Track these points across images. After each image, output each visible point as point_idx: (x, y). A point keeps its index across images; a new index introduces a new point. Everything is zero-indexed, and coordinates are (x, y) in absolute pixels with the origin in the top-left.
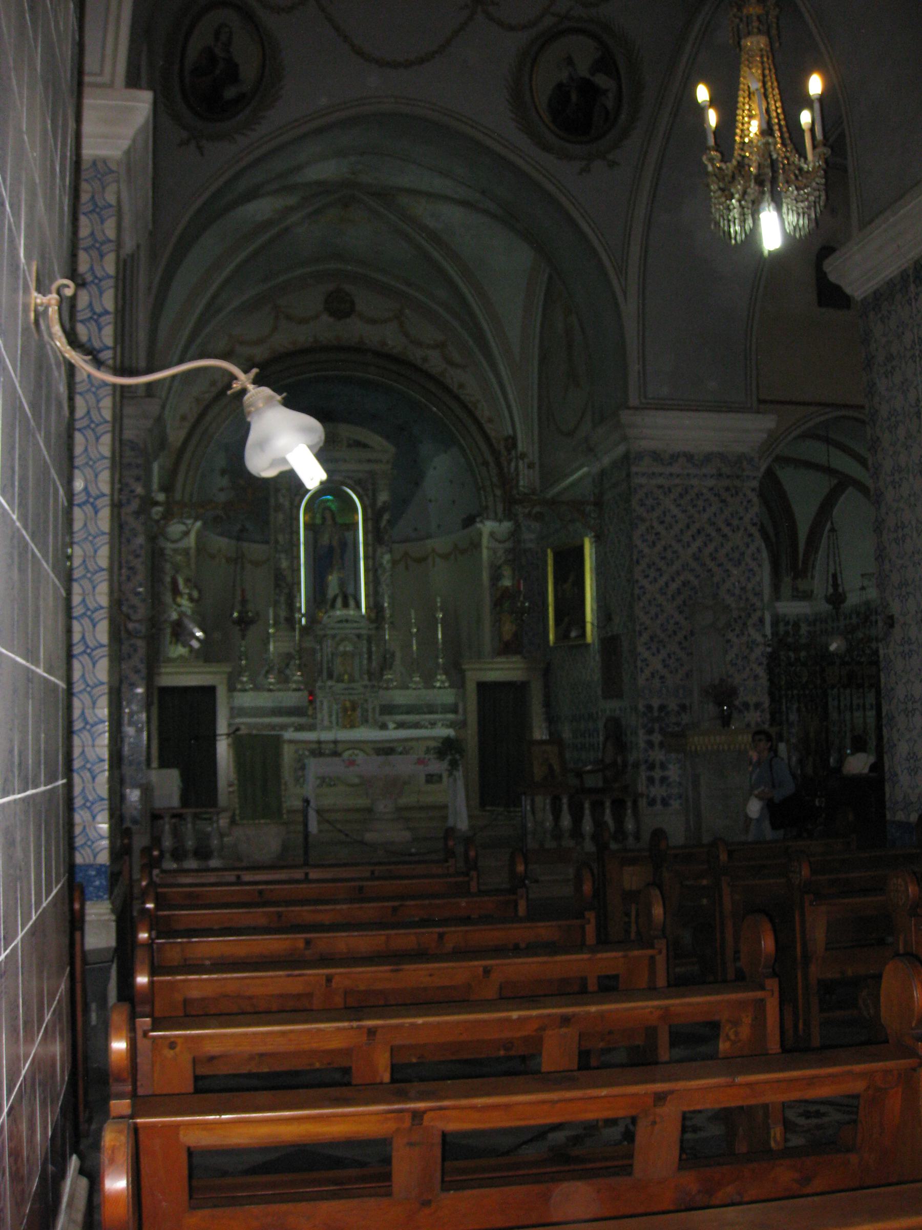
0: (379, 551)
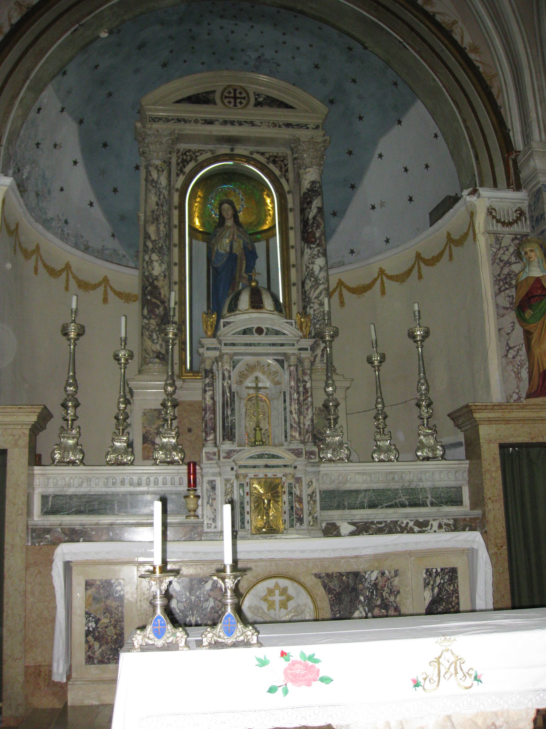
0: (307, 251)
